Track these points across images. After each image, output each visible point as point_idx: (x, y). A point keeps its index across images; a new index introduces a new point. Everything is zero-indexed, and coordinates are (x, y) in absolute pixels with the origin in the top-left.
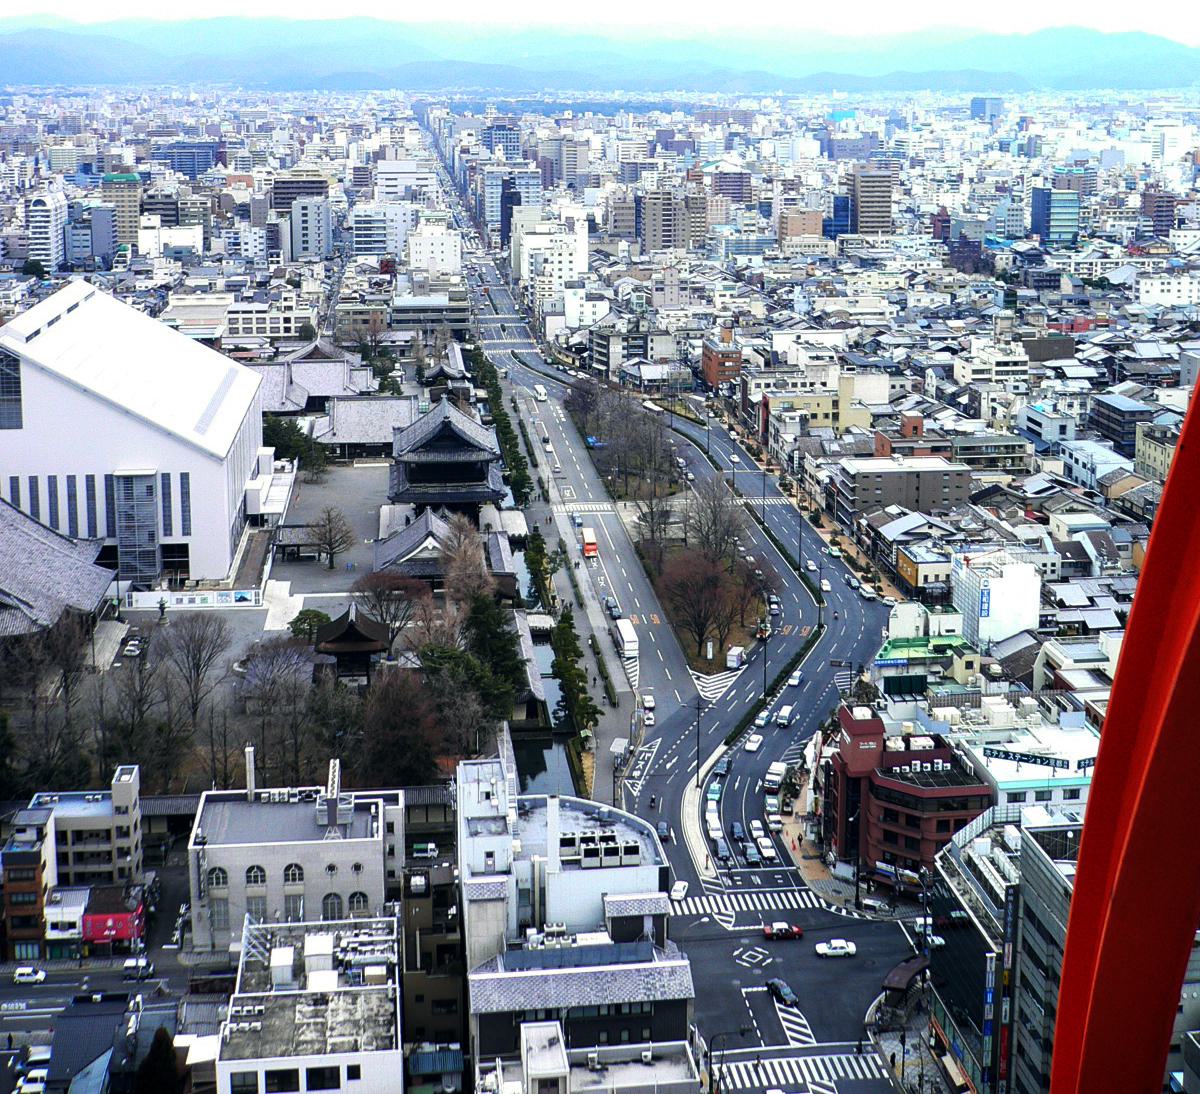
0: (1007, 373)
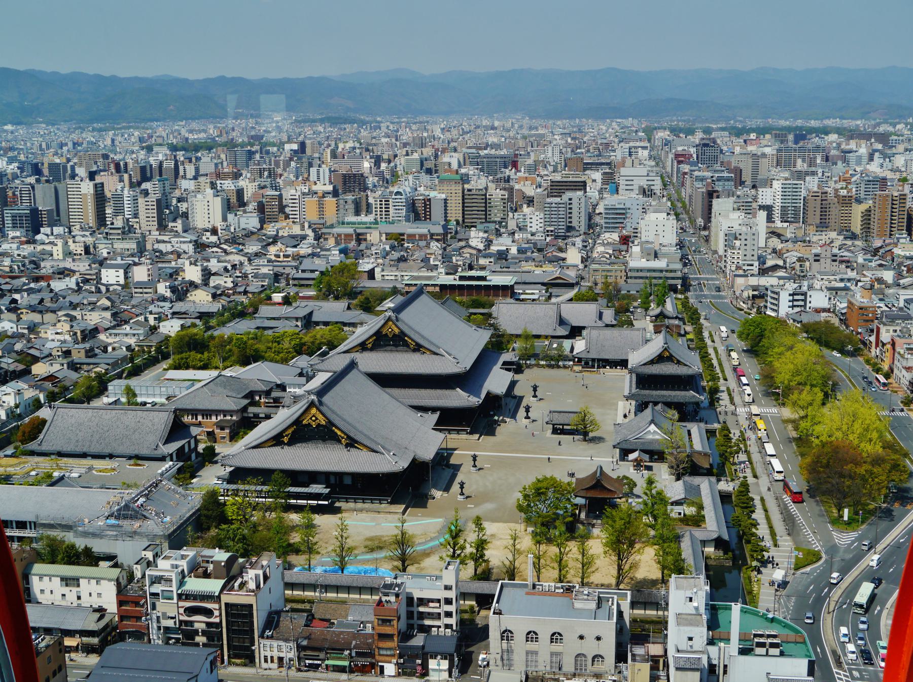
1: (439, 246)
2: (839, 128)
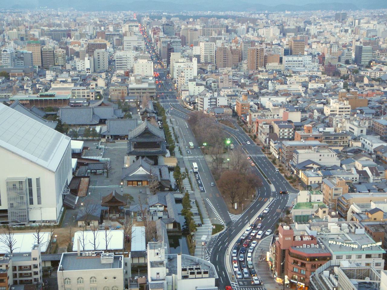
0: (342, 111)
2: (233, 16)
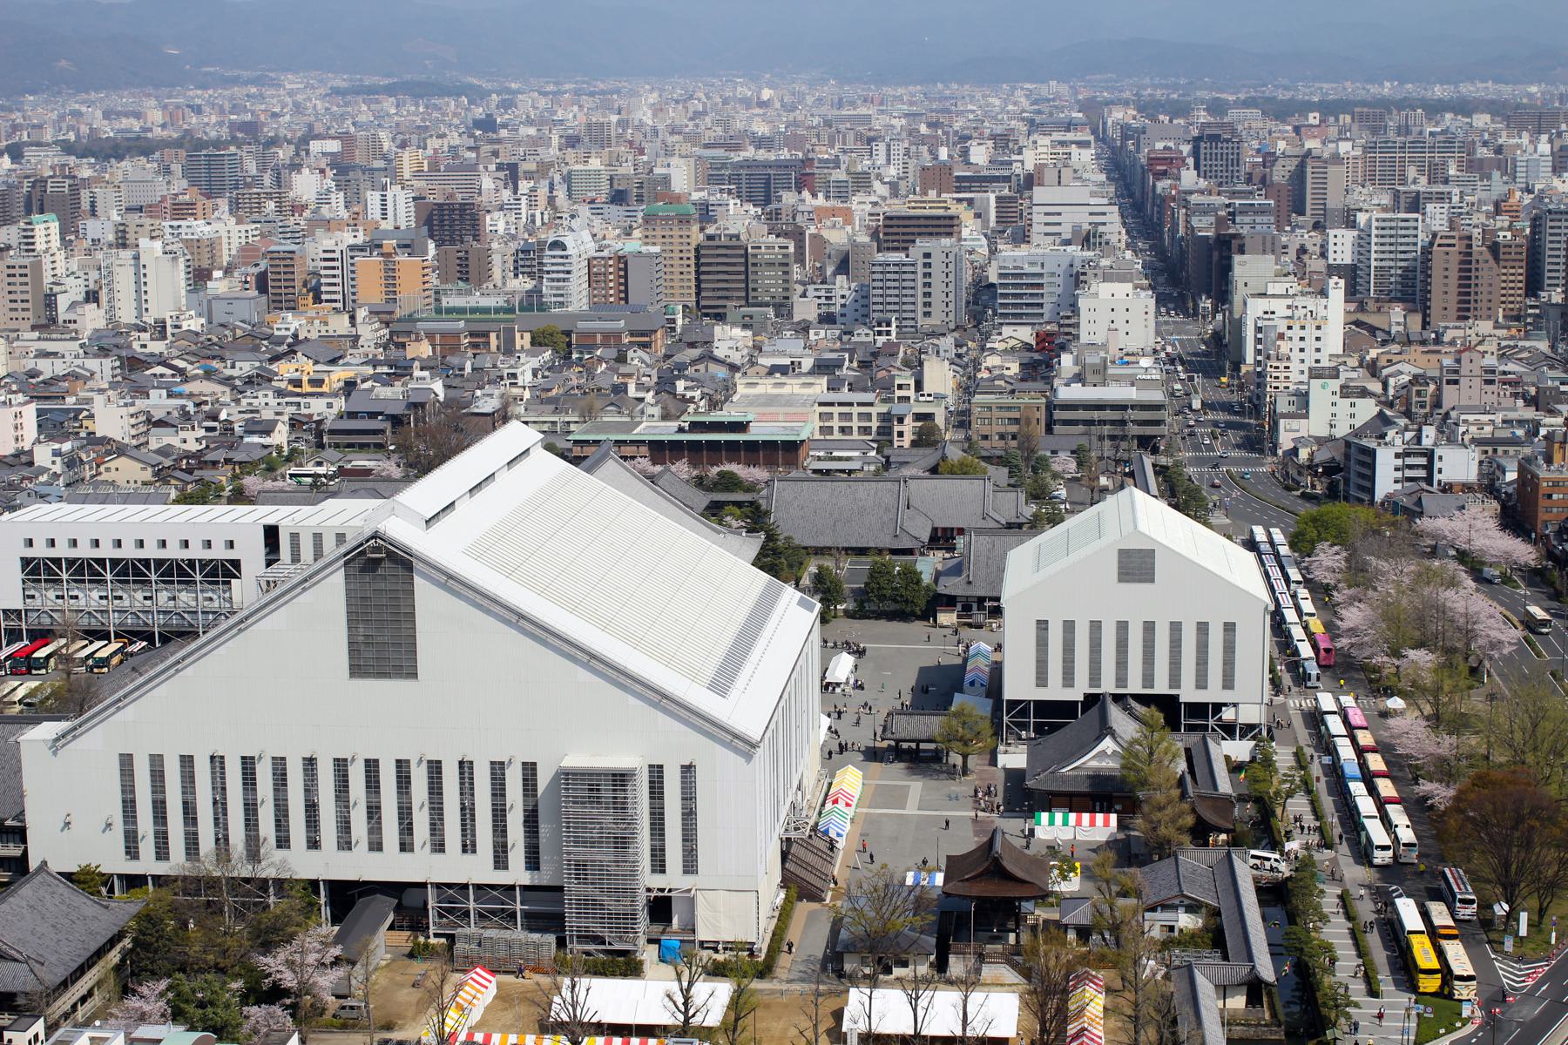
1: (646, 357)
2: (1493, 102)
